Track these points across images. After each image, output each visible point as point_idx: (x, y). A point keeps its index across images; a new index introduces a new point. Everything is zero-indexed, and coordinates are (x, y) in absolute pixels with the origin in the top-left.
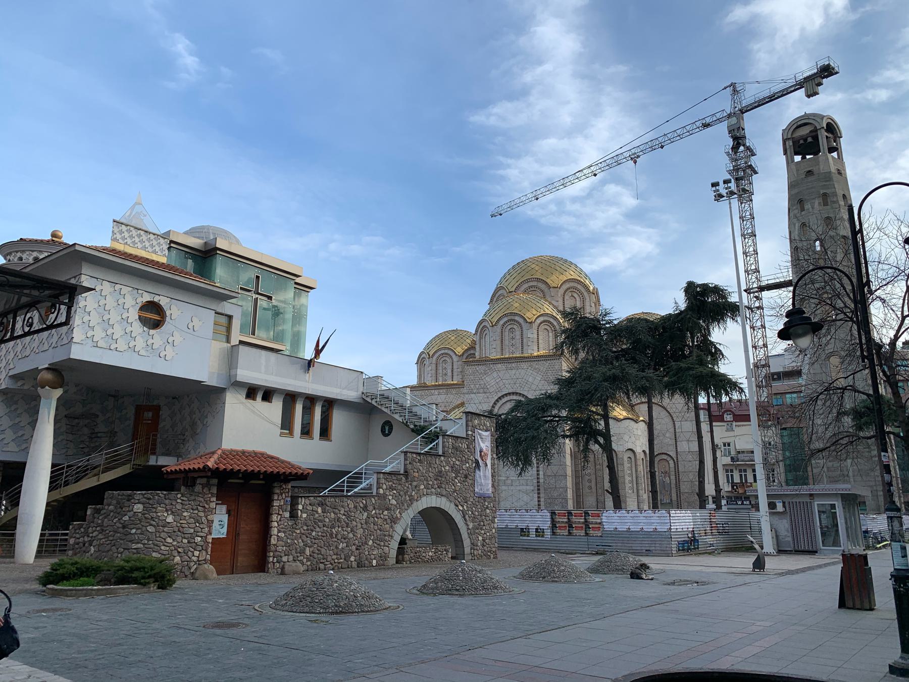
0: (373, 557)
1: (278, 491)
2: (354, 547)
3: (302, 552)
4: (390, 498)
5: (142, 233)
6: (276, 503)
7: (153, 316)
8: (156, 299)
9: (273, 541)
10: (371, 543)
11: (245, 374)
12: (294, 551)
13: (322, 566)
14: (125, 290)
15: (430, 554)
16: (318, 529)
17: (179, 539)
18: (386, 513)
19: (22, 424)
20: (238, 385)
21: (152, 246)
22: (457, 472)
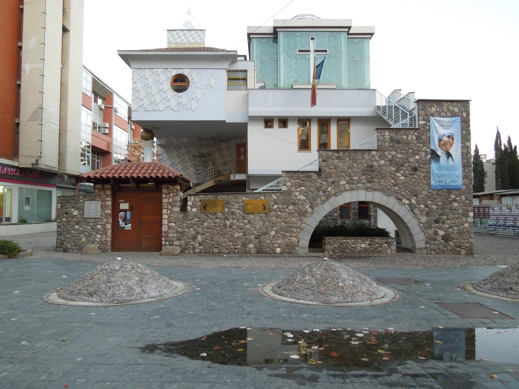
0: (276, 245)
1: (166, 192)
2: (252, 237)
3: (194, 238)
5: (186, 32)
6: (164, 201)
7: (180, 83)
8: (180, 72)
9: (164, 229)
10: (273, 233)
11: (256, 110)
12: (186, 237)
13: (216, 250)
14: (159, 71)
15: (363, 245)
16: (210, 221)
17: (84, 226)
18: (291, 207)
19: (176, 163)
20: (254, 119)
21: (194, 38)
22: (399, 166)
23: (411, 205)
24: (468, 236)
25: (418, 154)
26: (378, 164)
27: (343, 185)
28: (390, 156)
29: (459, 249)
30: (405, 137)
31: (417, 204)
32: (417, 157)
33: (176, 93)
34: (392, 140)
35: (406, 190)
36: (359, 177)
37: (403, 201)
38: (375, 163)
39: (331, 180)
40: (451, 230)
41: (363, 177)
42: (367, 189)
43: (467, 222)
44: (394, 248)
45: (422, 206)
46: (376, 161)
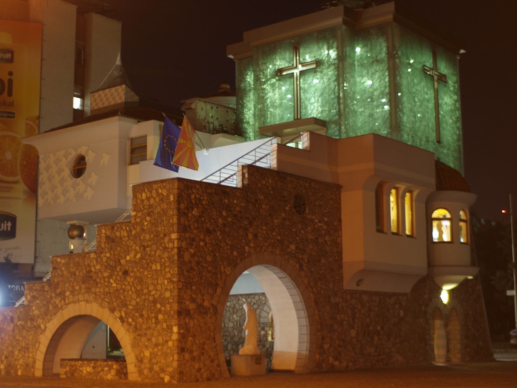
4: (34, 308)
21: (114, 99)
23: (121, 318)
24: (171, 358)
25: (128, 255)
26: (96, 269)
27: (68, 297)
28: (104, 260)
29: (162, 375)
30: (118, 234)
31: (125, 317)
32: (128, 258)
33: (74, 179)
34: (108, 237)
35: (117, 300)
36: (80, 287)
37: (115, 314)
38: (93, 270)
39: (58, 291)
40: (156, 349)
41: (83, 286)
42: (87, 301)
43: (171, 340)
44: (113, 372)
45: (130, 320)
46: (94, 266)
